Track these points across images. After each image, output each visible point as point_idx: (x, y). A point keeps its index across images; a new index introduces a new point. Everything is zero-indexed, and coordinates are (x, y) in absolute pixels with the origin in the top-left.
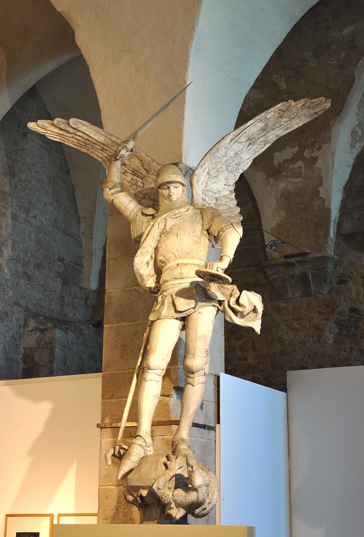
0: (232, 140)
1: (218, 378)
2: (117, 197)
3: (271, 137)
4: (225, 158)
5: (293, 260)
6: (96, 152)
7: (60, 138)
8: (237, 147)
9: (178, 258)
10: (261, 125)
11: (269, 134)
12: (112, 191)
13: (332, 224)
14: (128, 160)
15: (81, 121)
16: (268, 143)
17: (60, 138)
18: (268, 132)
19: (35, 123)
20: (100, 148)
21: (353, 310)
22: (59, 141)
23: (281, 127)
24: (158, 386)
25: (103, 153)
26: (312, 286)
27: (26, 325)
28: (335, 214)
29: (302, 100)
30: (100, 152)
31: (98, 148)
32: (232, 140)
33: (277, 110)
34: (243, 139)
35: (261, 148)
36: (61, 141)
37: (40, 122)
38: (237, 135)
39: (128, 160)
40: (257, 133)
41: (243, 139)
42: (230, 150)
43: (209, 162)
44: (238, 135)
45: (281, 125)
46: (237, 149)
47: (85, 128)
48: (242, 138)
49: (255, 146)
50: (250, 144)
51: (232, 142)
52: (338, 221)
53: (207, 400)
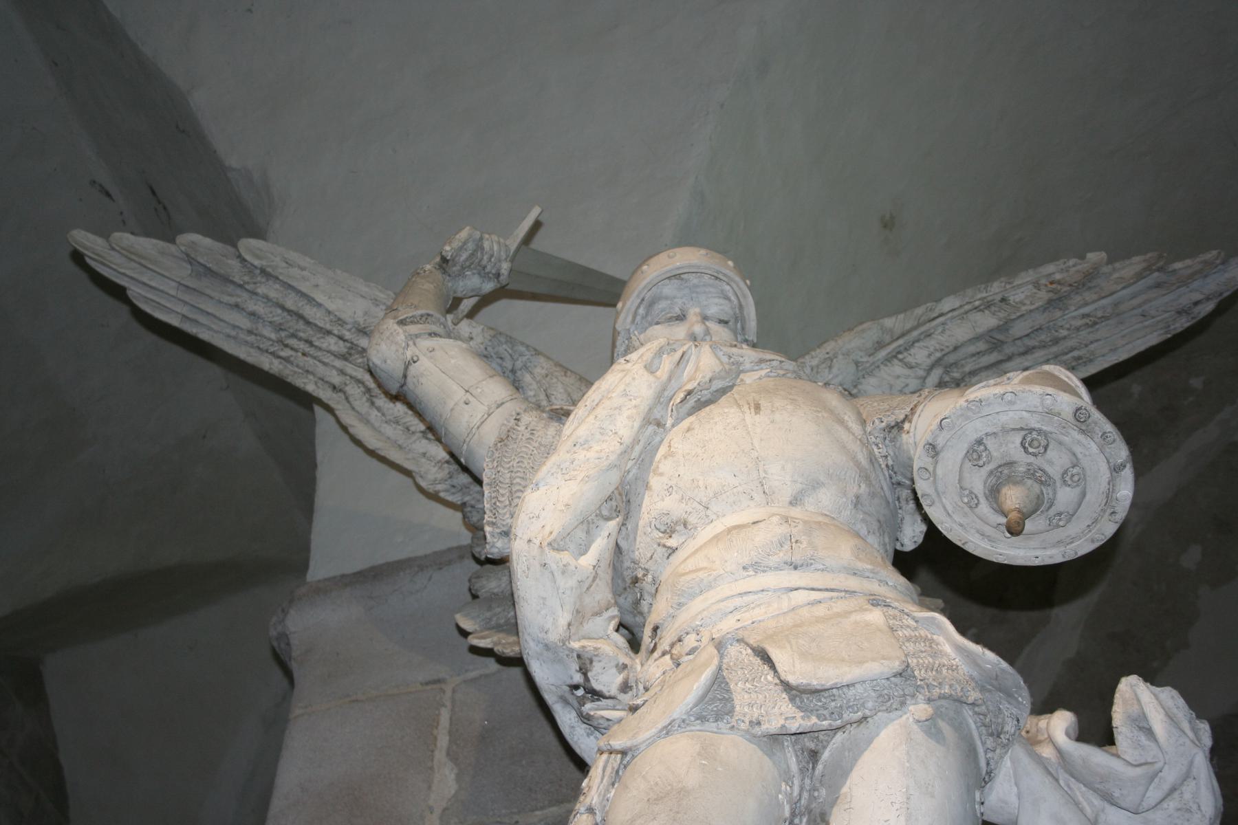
0: (880, 345)
6: (321, 370)
7: (185, 310)
9: (758, 497)
10: (987, 321)
12: (413, 329)
17: (185, 310)
20: (341, 347)
23: (1054, 349)
25: (350, 369)
29: (1136, 259)
30: (338, 363)
31: (333, 348)
32: (880, 345)
33: (1043, 281)
34: (920, 355)
38: (898, 332)
40: (972, 349)
41: (920, 355)
42: (872, 381)
44: (903, 335)
45: (1056, 341)
47: (295, 271)
48: (912, 351)
51: (883, 354)
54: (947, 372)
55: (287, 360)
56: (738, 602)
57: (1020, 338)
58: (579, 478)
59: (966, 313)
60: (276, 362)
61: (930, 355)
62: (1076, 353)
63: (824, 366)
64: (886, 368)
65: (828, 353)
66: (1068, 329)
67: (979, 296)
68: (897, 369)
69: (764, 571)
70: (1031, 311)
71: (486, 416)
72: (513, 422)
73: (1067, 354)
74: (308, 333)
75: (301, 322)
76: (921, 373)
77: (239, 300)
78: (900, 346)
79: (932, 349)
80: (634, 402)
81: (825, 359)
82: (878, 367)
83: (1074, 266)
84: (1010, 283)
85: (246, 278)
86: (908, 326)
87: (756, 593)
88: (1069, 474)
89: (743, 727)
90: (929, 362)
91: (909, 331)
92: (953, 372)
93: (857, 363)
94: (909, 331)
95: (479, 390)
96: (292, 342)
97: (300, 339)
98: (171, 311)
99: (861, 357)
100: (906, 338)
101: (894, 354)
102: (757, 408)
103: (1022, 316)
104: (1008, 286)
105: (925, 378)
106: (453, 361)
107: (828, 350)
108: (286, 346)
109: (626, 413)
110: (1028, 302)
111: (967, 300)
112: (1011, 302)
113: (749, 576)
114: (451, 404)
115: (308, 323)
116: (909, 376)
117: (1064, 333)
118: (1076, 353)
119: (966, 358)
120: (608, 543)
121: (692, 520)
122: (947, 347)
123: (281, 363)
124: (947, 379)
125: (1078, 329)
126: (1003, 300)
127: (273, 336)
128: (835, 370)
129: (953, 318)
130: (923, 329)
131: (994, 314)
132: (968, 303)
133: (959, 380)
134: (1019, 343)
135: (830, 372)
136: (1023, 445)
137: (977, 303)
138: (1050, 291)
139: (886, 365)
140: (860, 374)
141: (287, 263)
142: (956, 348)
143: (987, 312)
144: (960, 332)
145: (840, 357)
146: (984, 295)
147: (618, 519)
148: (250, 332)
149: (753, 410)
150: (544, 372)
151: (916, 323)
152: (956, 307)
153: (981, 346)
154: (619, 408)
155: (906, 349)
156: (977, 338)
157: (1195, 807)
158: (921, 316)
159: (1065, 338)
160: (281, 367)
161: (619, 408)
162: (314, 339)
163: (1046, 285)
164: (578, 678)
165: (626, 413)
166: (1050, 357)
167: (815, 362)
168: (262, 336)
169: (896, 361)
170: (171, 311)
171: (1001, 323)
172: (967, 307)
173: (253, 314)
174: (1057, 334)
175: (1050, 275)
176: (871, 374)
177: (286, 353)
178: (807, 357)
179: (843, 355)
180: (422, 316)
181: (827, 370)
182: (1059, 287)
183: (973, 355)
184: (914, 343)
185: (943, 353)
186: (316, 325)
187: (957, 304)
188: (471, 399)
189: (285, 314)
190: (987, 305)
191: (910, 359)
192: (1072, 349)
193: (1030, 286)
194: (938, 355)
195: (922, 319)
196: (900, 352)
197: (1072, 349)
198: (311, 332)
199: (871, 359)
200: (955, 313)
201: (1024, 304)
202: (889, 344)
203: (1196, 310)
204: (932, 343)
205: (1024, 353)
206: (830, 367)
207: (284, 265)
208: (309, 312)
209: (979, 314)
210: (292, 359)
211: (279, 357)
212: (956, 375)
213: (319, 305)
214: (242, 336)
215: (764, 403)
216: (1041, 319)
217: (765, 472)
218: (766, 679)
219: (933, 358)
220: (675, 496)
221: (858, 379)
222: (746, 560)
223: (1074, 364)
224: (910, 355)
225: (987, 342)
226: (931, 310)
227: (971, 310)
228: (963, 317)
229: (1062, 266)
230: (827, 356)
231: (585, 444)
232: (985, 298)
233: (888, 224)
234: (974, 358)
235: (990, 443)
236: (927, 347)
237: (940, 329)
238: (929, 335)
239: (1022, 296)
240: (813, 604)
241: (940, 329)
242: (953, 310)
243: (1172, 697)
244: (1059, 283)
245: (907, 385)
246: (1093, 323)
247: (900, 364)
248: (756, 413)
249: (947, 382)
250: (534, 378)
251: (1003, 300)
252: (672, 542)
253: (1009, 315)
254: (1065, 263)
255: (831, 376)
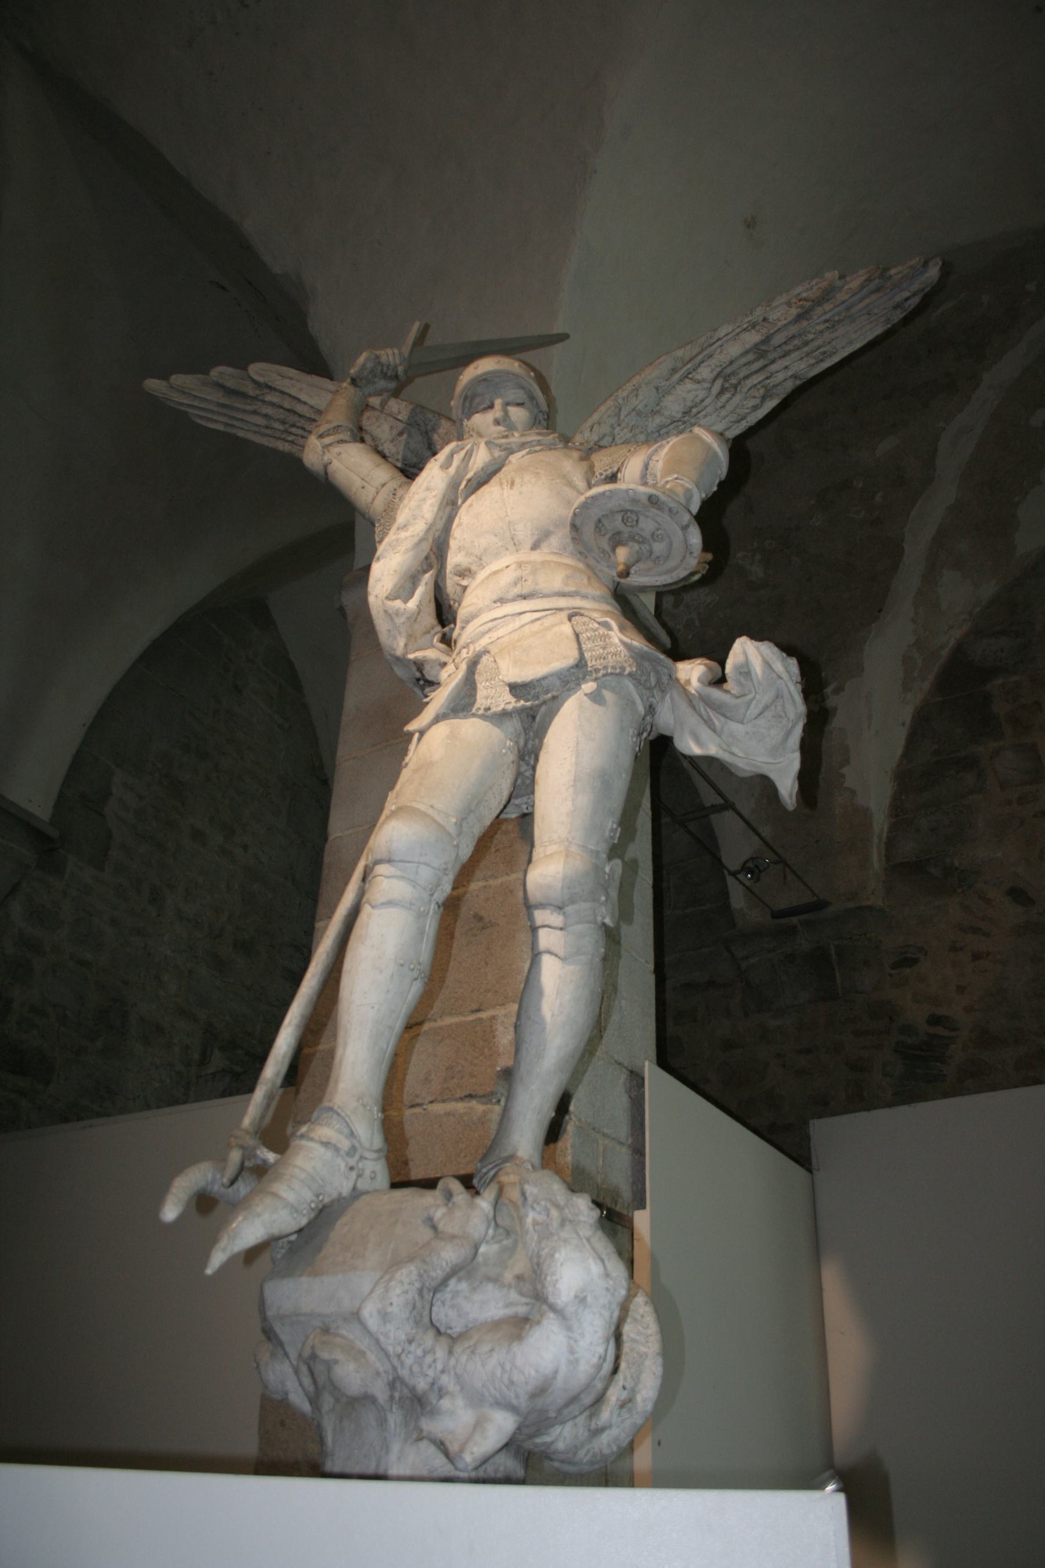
0: (674, 371)
1: (636, 1078)
2: (339, 454)
3: (780, 377)
4: (658, 420)
5: (795, 920)
7: (225, 420)
8: (687, 392)
10: (753, 338)
11: (773, 368)
12: (327, 440)
13: (875, 840)
14: (392, 441)
15: (277, 367)
16: (771, 397)
17: (225, 420)
18: (773, 362)
19: (164, 383)
21: (935, 1020)
22: (221, 428)
23: (806, 349)
24: (421, 932)
26: (838, 975)
27: (204, 1061)
28: (880, 822)
29: (861, 272)
32: (674, 371)
33: (794, 300)
34: (705, 372)
35: (755, 408)
36: (229, 430)
37: (178, 379)
39: (392, 441)
40: (744, 360)
41: (705, 372)
42: (670, 398)
43: (613, 421)
45: (806, 343)
46: (690, 397)
47: (287, 382)
48: (699, 370)
49: (738, 398)
50: (723, 391)
51: (677, 376)
52: (888, 838)
53: (606, 1131)
54: (726, 380)
55: (292, 442)
56: (490, 625)
57: (780, 346)
58: (401, 552)
59: (738, 334)
60: (287, 444)
61: (712, 371)
62: (822, 350)
63: (632, 395)
64: (680, 387)
65: (634, 385)
66: (814, 334)
67: (747, 320)
68: (689, 385)
69: (506, 603)
70: (785, 325)
71: (375, 494)
72: (391, 496)
73: (815, 351)
74: (302, 422)
75: (296, 416)
76: (707, 385)
77: (256, 407)
78: (688, 369)
79: (713, 366)
80: (434, 494)
81: (633, 390)
82: (674, 387)
83: (816, 285)
84: (769, 306)
85: (258, 392)
86: (694, 353)
87: (501, 618)
88: (656, 535)
89: (481, 712)
90: (712, 376)
91: (695, 356)
92: (731, 380)
93: (657, 388)
94: (695, 356)
95: (370, 477)
96: (294, 430)
97: (298, 427)
98: (216, 421)
99: (660, 383)
100: (693, 362)
101: (686, 374)
102: (513, 484)
103: (779, 329)
104: (768, 309)
105: (710, 388)
106: (353, 459)
107: (635, 383)
108: (291, 433)
109: (429, 502)
110: (783, 319)
111: (738, 324)
112: (771, 320)
113: (497, 607)
114: (354, 489)
115: (300, 416)
116: (698, 389)
117: (811, 337)
118: (822, 350)
119: (740, 368)
120: (426, 589)
121: (474, 568)
122: (725, 363)
123: (289, 445)
124: (727, 385)
125: (821, 332)
126: (765, 319)
127: (281, 428)
128: (640, 397)
129: (727, 341)
130: (705, 353)
131: (758, 332)
132: (739, 327)
133: (736, 384)
134: (779, 350)
135: (637, 399)
136: (623, 520)
137: (745, 326)
138: (799, 307)
139: (680, 385)
140: (661, 395)
141: (281, 376)
142: (731, 363)
143: (753, 331)
144: (734, 350)
145: (644, 386)
146: (750, 318)
147: (431, 572)
148: (267, 427)
149: (509, 486)
150: (444, 431)
151: (700, 350)
152: (730, 331)
153: (751, 357)
154: (424, 500)
155: (694, 370)
156: (747, 352)
157: (783, 715)
158: (703, 344)
159: (813, 340)
160: (290, 447)
161: (424, 500)
162: (306, 426)
163: (796, 303)
164: (418, 675)
165: (429, 502)
166: (803, 355)
167: (625, 394)
168: (275, 429)
169: (687, 380)
170: (216, 421)
171: (764, 338)
172: (739, 330)
173: (266, 416)
174: (806, 338)
175: (799, 294)
176: (669, 393)
177: (290, 438)
178: (620, 391)
179: (646, 384)
180: (334, 428)
181: (634, 399)
182: (805, 303)
183: (745, 365)
184: (700, 364)
185: (722, 367)
186: (305, 416)
187: (730, 329)
188: (365, 484)
189: (286, 412)
190: (753, 326)
191: (698, 377)
192: (819, 348)
193: (784, 306)
194: (719, 369)
195: (705, 345)
196: (690, 373)
197: (819, 348)
198: (303, 422)
199: (668, 383)
200: (729, 337)
201: (780, 321)
202: (681, 369)
203: (907, 305)
204: (713, 362)
205: (784, 356)
206: (637, 396)
207: (279, 378)
208: (300, 409)
209: (747, 333)
210: (296, 441)
211: (287, 441)
212: (734, 381)
213: (305, 403)
214: (263, 430)
215: (518, 480)
216: (793, 330)
217: (515, 530)
218: (498, 678)
219: (715, 373)
220: (463, 553)
221: (660, 399)
222: (495, 597)
223: (821, 358)
224: (698, 373)
225: (754, 353)
226: (711, 337)
227: (741, 332)
228: (735, 339)
229: (808, 286)
230: (634, 388)
231: (404, 527)
232: (750, 321)
233: (750, 224)
234: (747, 367)
235: (605, 522)
236: (709, 366)
237: (719, 351)
238: (711, 356)
239: (779, 314)
240: (533, 621)
241: (719, 351)
242: (727, 334)
243: (770, 647)
244: (805, 300)
245: (697, 396)
246: (832, 325)
247: (690, 381)
248: (511, 488)
249: (728, 387)
250: (439, 436)
251: (765, 319)
252: (464, 583)
253: (769, 331)
254: (809, 283)
255: (638, 402)
